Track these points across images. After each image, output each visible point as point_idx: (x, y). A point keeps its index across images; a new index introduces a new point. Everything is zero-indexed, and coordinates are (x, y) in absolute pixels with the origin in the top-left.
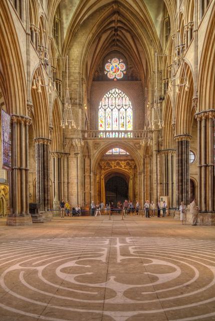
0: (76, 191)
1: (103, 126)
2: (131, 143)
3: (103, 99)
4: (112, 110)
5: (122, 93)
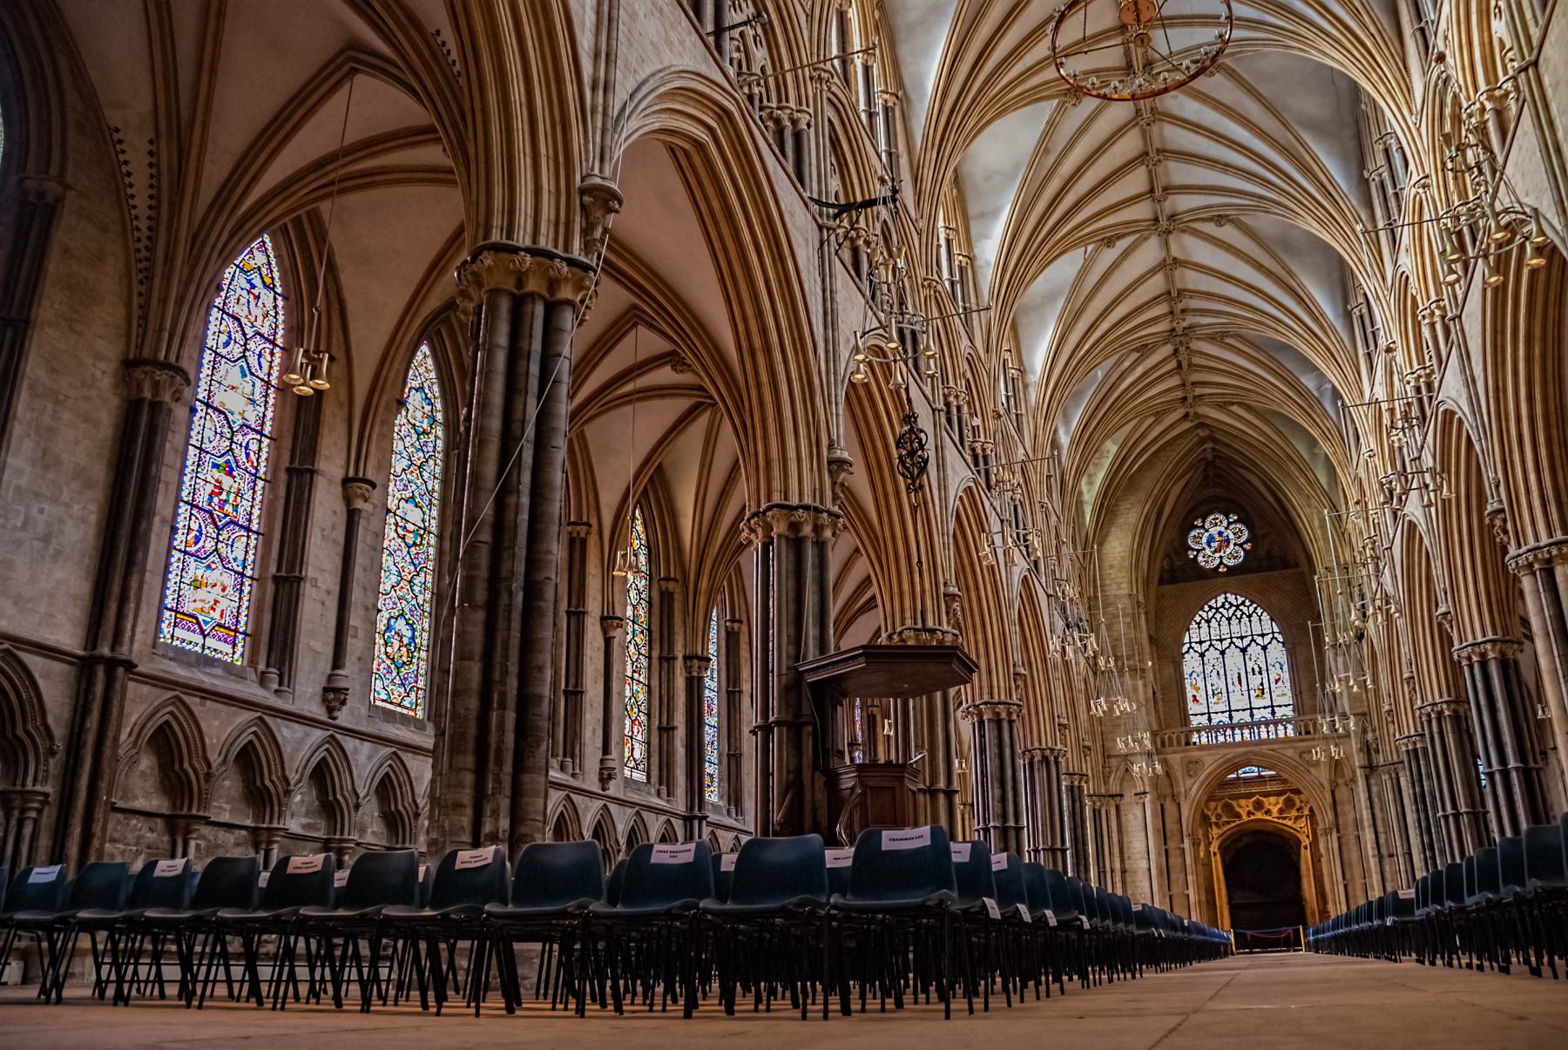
1: (1201, 697)
2: (1290, 753)
3: (1194, 625)
4: (1223, 653)
5: (1247, 603)
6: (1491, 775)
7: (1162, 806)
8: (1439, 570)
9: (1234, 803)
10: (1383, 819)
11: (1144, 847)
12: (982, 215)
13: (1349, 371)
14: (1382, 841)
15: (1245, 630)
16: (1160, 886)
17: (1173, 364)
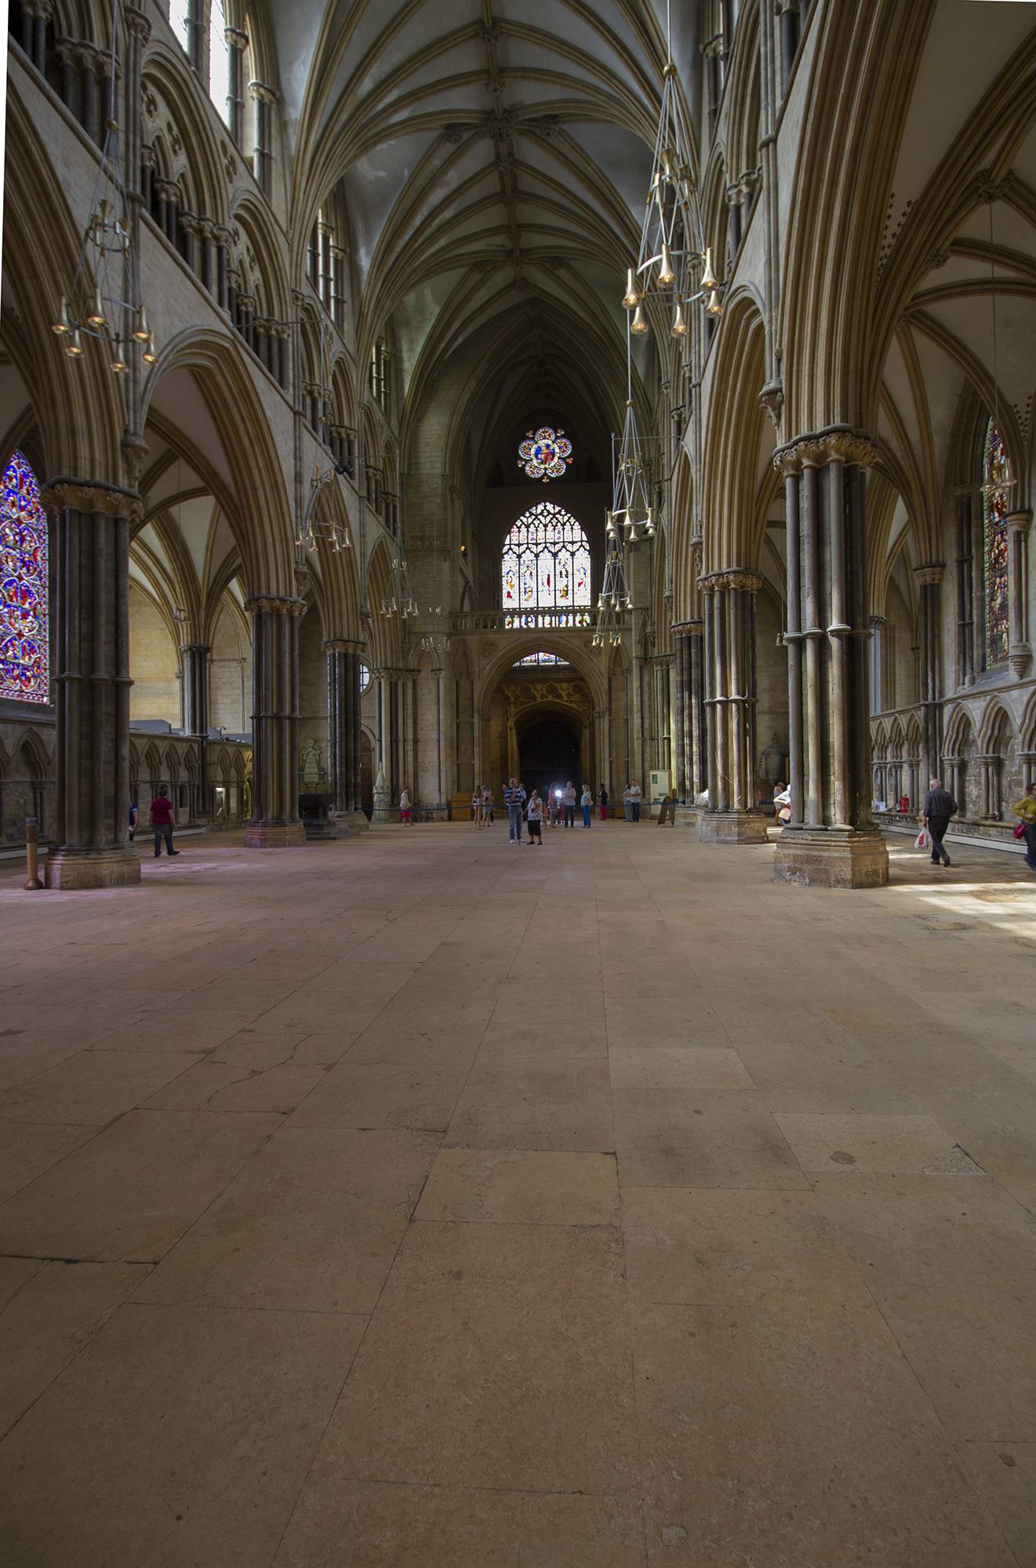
0: (436, 759)
3: (515, 529)
4: (537, 556)
5: (563, 513)
7: (457, 683)
9: (531, 687)
10: (650, 706)
11: (435, 719)
14: (647, 725)
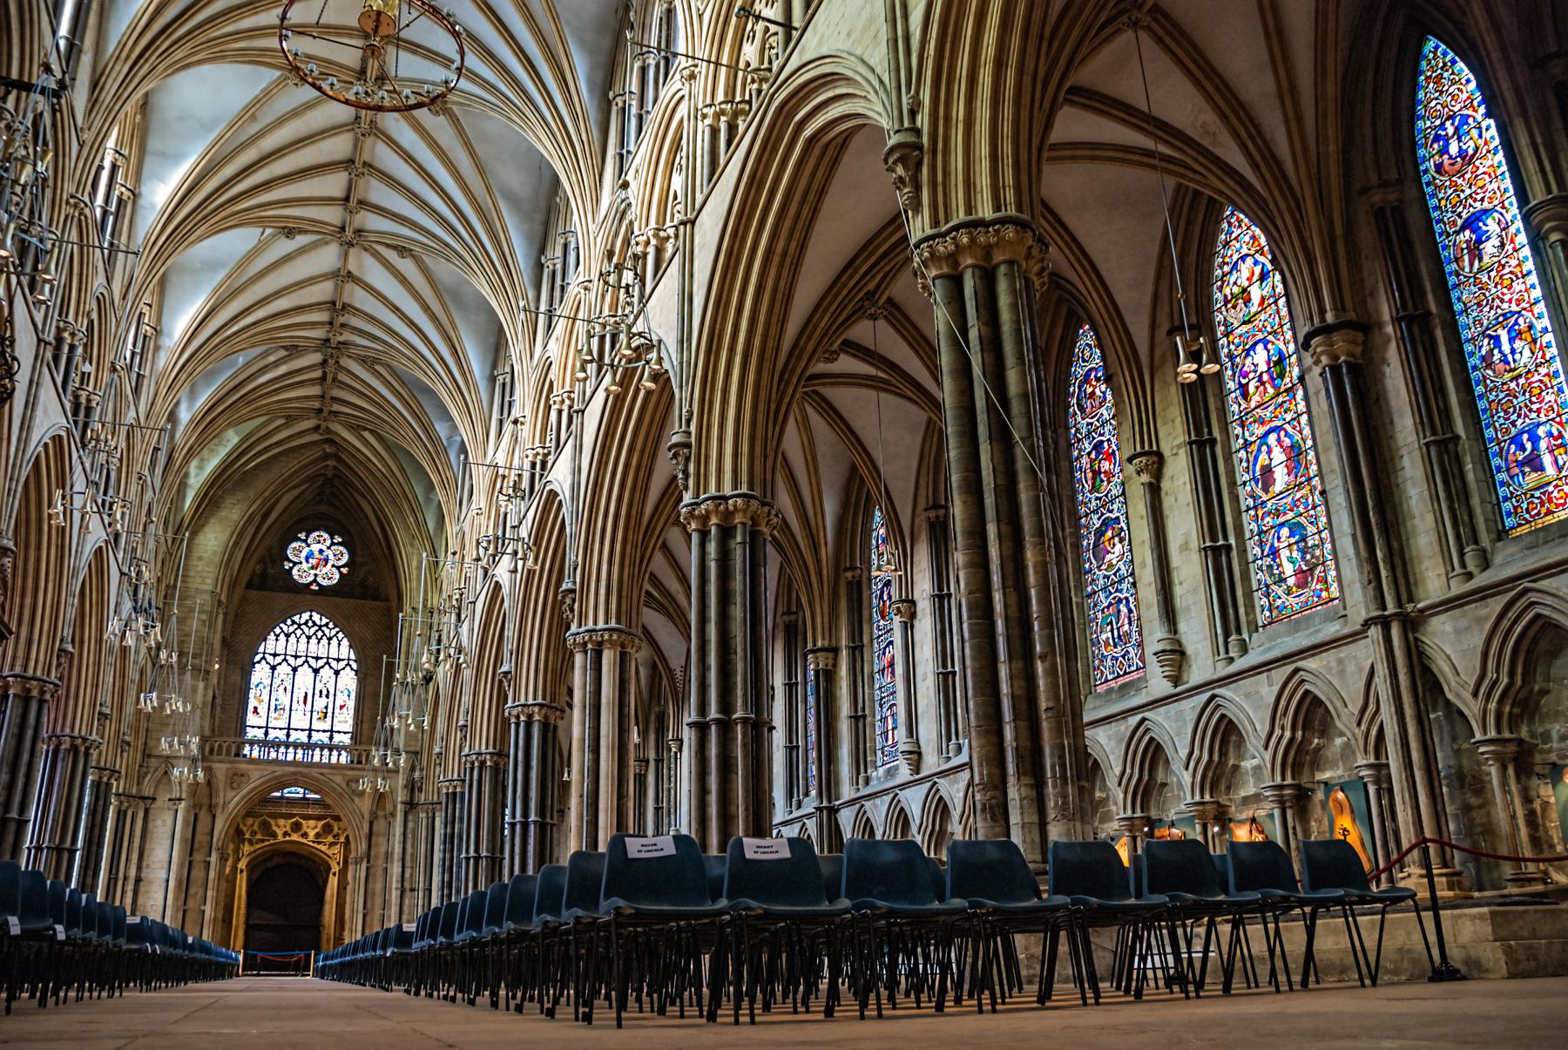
1: (263, 710)
2: (339, 779)
3: (272, 637)
4: (295, 670)
5: (331, 625)
6: (513, 825)
8: (511, 632)
9: (272, 822)
10: (412, 855)
11: (166, 856)
12: (163, 155)
13: (479, 430)
14: (407, 875)
15: (322, 652)
16: (176, 899)
17: (318, 374)
